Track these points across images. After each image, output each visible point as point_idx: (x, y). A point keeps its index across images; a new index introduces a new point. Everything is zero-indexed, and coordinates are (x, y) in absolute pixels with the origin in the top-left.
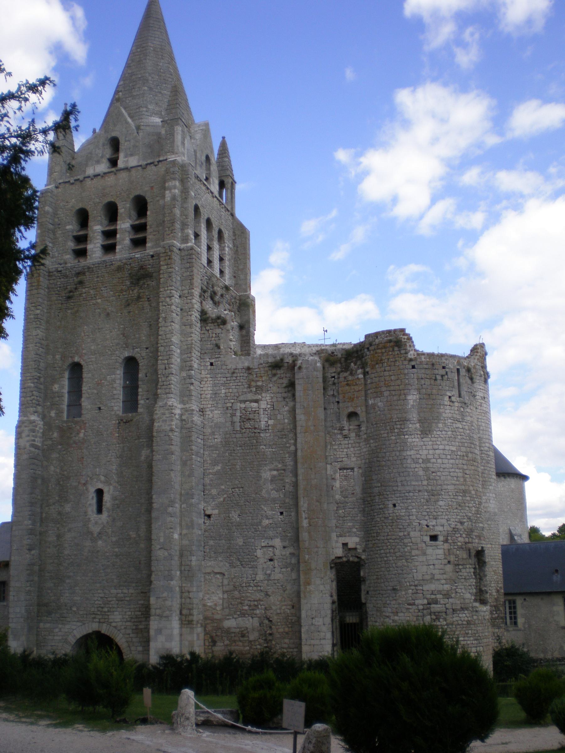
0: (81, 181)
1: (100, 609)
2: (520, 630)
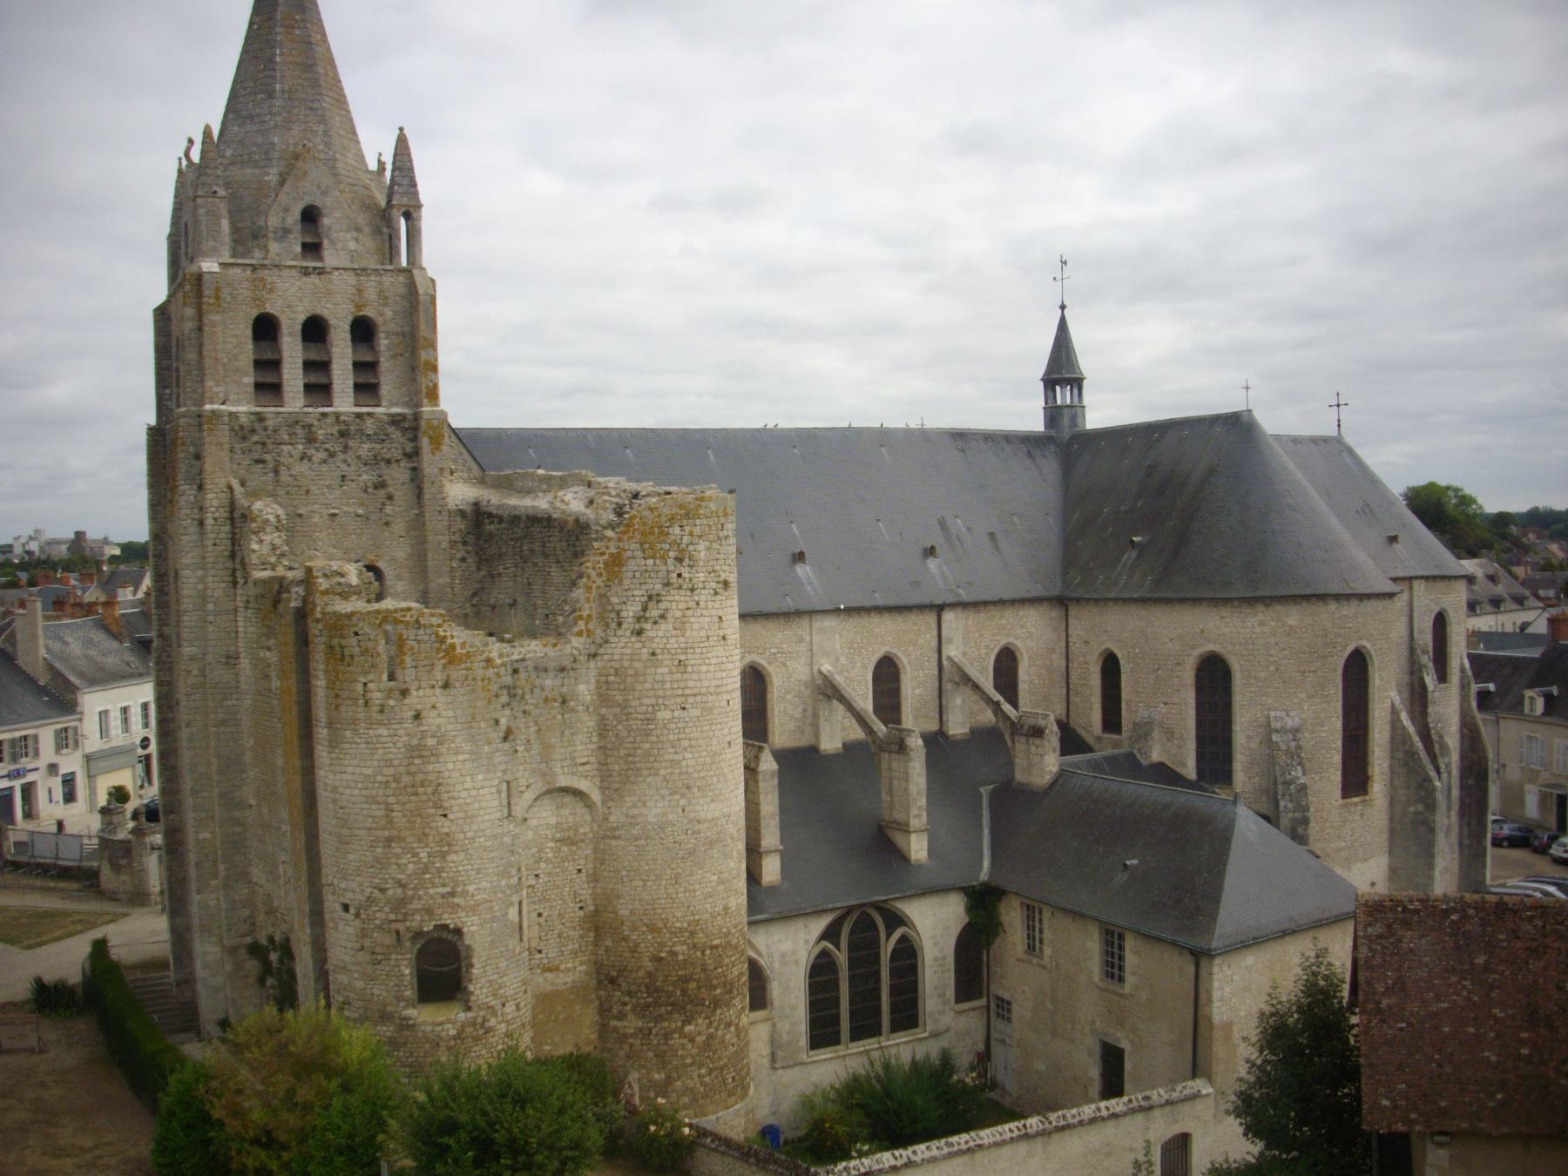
2: (1043, 967)
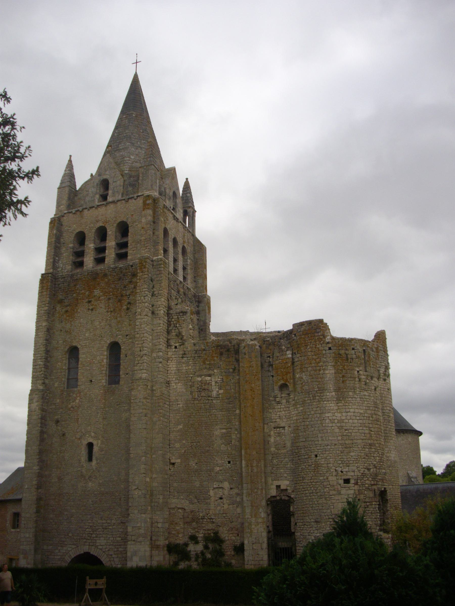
0: (81, 212)
1: (90, 535)
